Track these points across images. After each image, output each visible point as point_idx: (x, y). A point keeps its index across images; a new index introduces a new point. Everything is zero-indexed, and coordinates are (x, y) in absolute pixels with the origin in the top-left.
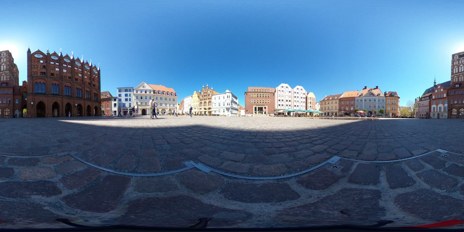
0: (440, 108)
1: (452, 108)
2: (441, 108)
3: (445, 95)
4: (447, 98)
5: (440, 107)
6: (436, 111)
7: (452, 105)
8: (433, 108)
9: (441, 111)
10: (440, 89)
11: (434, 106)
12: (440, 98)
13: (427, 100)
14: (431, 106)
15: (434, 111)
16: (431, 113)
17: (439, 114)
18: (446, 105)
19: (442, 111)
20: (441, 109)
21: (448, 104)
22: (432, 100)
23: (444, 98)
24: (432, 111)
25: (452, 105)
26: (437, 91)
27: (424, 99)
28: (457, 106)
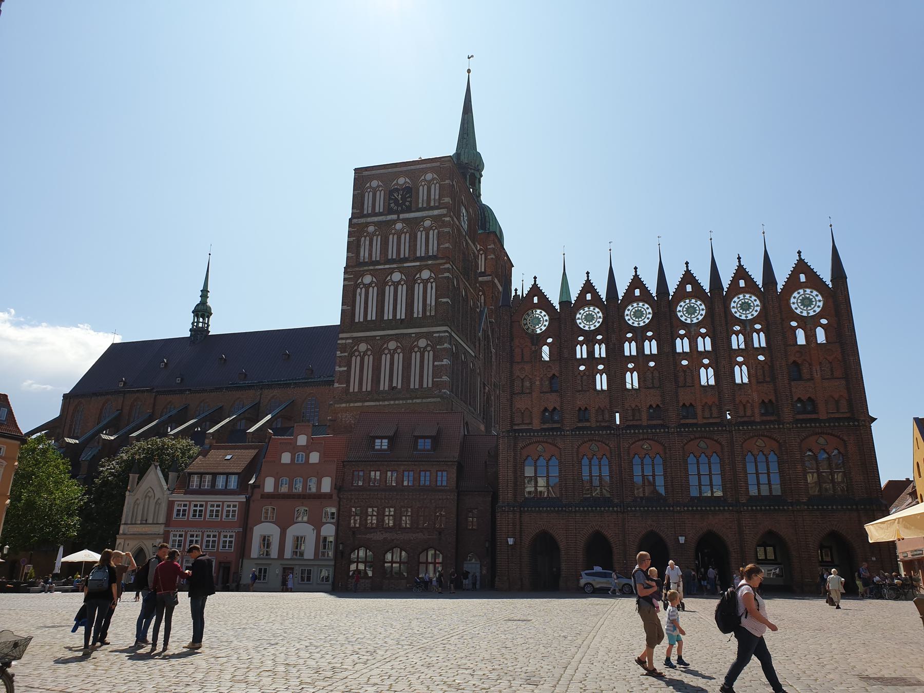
0: (299, 540)
3: (327, 485)
4: (335, 497)
6: (274, 553)
9: (302, 554)
10: (308, 449)
12: (304, 497)
13: (226, 492)
22: (257, 496)
24: (255, 551)
25: (354, 533)
26: (293, 459)
27: (207, 485)
28: (378, 536)
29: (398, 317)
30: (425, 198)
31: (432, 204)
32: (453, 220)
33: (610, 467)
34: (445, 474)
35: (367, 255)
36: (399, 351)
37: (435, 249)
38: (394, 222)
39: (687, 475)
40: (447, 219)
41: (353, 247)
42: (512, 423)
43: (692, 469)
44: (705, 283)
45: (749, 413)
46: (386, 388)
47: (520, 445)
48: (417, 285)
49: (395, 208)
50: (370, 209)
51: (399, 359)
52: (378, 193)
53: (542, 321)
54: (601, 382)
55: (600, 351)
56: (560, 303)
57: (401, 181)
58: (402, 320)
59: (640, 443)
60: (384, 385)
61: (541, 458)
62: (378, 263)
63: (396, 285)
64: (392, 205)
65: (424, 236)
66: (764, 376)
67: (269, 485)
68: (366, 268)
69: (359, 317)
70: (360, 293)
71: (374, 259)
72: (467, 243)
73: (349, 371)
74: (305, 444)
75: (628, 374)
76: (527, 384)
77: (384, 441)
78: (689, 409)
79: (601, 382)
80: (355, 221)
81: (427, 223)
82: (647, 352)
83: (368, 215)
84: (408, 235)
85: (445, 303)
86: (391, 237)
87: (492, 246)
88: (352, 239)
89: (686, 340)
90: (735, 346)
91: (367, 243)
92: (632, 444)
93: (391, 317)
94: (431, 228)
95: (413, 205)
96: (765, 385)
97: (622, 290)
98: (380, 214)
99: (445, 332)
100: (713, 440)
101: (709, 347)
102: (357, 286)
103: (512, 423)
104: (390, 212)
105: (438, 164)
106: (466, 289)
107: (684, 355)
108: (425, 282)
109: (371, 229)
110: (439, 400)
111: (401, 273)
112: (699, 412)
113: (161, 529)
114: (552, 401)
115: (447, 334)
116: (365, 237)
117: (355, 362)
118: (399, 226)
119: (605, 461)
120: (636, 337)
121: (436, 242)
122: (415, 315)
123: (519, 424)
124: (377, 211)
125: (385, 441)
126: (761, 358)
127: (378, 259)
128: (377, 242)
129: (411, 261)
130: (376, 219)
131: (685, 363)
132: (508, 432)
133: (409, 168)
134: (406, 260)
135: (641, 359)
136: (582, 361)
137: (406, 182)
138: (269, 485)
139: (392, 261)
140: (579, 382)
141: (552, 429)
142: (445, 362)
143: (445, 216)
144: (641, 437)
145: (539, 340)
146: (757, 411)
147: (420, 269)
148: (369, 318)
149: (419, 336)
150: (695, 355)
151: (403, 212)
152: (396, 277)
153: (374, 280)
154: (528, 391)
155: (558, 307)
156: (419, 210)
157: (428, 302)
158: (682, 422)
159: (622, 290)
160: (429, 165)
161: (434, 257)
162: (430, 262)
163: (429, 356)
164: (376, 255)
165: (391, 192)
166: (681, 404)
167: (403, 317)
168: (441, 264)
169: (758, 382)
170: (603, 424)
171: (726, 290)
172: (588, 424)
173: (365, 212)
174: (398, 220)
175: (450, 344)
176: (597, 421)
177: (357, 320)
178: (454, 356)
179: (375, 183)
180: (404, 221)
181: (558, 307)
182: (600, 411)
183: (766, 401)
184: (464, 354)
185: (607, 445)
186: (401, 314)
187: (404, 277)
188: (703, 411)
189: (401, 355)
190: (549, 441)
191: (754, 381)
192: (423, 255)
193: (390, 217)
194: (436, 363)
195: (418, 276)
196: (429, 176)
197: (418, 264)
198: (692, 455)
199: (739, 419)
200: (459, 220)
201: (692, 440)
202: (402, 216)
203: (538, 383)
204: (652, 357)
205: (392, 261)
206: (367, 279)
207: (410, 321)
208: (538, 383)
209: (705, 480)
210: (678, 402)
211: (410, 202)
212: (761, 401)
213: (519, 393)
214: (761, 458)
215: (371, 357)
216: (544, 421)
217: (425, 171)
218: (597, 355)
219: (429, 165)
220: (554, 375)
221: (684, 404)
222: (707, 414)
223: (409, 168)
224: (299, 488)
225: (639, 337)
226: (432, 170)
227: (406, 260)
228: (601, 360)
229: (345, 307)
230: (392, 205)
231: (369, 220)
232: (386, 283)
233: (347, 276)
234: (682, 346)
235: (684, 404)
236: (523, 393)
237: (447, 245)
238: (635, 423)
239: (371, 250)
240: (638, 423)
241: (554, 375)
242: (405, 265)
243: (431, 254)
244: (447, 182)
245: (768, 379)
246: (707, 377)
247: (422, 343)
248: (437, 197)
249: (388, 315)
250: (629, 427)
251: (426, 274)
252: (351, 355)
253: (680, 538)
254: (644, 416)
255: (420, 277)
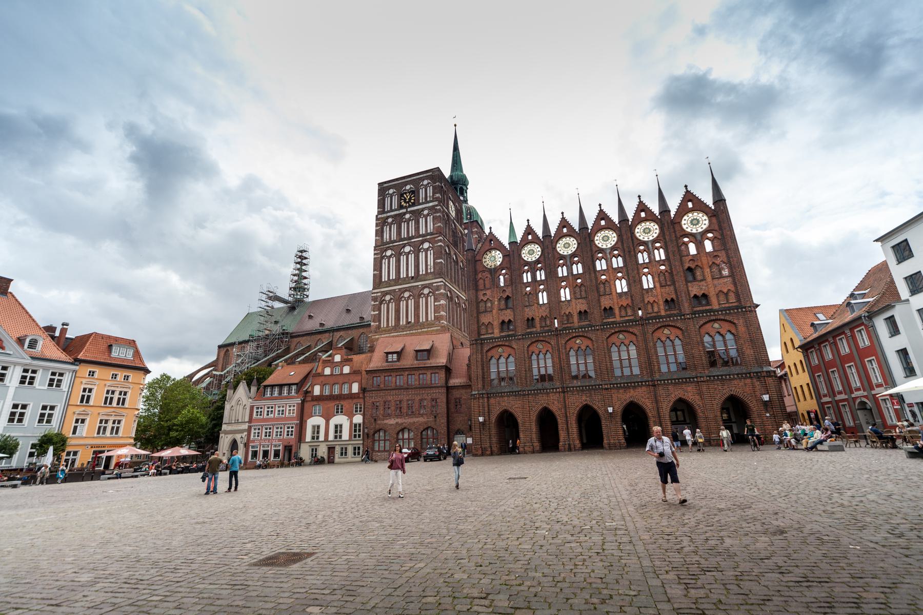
0: (339, 429)
1: (377, 427)
2: (341, 426)
3: (355, 388)
4: (361, 396)
5: (336, 426)
6: (322, 438)
7: (375, 420)
8: (314, 427)
9: (341, 437)
11: (315, 421)
14: (306, 421)
15: (315, 437)
16: (302, 444)
17: (334, 447)
18: (358, 419)
19: (343, 438)
20: (341, 432)
21: (364, 415)
22: (309, 399)
23: (351, 396)
24: (308, 438)
25: (375, 420)
26: (332, 371)
29: (410, 275)
30: (424, 196)
31: (428, 199)
32: (443, 208)
33: (553, 359)
34: (437, 375)
35: (388, 237)
36: (411, 298)
37: (432, 228)
38: (405, 214)
39: (611, 361)
40: (439, 207)
41: (379, 233)
42: (479, 334)
43: (615, 356)
44: (615, 218)
45: (656, 309)
46: (404, 323)
47: (486, 348)
48: (421, 253)
49: (405, 205)
50: (389, 207)
51: (411, 303)
52: (394, 197)
53: (495, 258)
54: (543, 298)
55: (541, 275)
56: (509, 244)
57: (408, 187)
58: (412, 278)
59: (573, 340)
60: (403, 322)
61: (502, 358)
62: (395, 241)
63: (408, 254)
64: (403, 203)
65: (424, 221)
66: (666, 281)
67: (317, 390)
68: (388, 246)
69: (385, 278)
70: (385, 262)
71: (392, 239)
72: (455, 225)
73: (380, 314)
74: (339, 360)
75: (562, 290)
76: (489, 305)
77: (394, 355)
78: (609, 311)
79: (543, 298)
80: (380, 216)
81: (426, 212)
82: (575, 272)
83: (388, 212)
84: (413, 222)
85: (439, 262)
86: (403, 224)
87: (476, 229)
88: (378, 228)
89: (603, 261)
90: (641, 261)
91: (388, 229)
92: (568, 340)
93: (405, 276)
94: (428, 215)
95: (416, 202)
96: (667, 287)
97: (553, 230)
98: (396, 210)
99: (441, 282)
100: (629, 332)
101: (621, 264)
102: (382, 258)
103: (479, 334)
104: (401, 207)
105: (431, 173)
106: (455, 254)
107: (603, 272)
108: (426, 250)
109: (390, 220)
110: (439, 328)
111: (410, 246)
112: (617, 311)
113: (245, 426)
114: (508, 315)
115: (442, 283)
116: (387, 226)
117: (384, 307)
118: (407, 216)
119: (549, 355)
120: (566, 262)
121: (432, 224)
122: (421, 273)
123: (484, 335)
124: (393, 208)
125: (396, 355)
126: (663, 268)
127: (395, 239)
128: (394, 228)
129: (416, 238)
130: (392, 213)
131: (604, 277)
132: (476, 340)
133: (412, 178)
134: (413, 237)
135: (572, 277)
136: (528, 284)
137: (411, 188)
138: (317, 390)
139: (405, 239)
140: (527, 299)
141: (509, 336)
142: (442, 302)
143: (437, 205)
144: (574, 335)
145: (495, 272)
146: (662, 307)
147: (422, 242)
148: (391, 278)
149: (424, 287)
150: (611, 270)
151: (410, 206)
152: (407, 249)
153: (393, 253)
154: (489, 310)
155: (508, 247)
156: (420, 204)
157: (429, 263)
158: (605, 321)
159: (553, 230)
160: (425, 175)
161: (431, 234)
162: (428, 237)
163: (431, 299)
164: (394, 236)
165: (402, 195)
166: (603, 308)
167: (413, 275)
168: (436, 237)
169: (661, 286)
170: (546, 329)
171: (631, 220)
172: (534, 330)
173: (386, 210)
174: (407, 212)
175: (445, 290)
176: (541, 327)
177: (383, 280)
178: (450, 299)
179: (391, 191)
180: (411, 212)
181: (508, 247)
182: (543, 319)
183: (669, 299)
184: (457, 297)
185: (549, 343)
186: (412, 273)
187: (412, 249)
188: (620, 311)
189: (413, 300)
190: (507, 344)
191: (658, 285)
192: (424, 233)
193: (401, 211)
194: (436, 304)
195: (421, 247)
196: (425, 182)
197: (421, 239)
198: (614, 345)
199: (649, 316)
200: (448, 209)
201: (613, 334)
202: (409, 210)
203: (496, 303)
204: (578, 276)
205: (405, 239)
206: (389, 253)
207: (417, 277)
208: (496, 303)
209: (626, 363)
210: (600, 306)
211: (414, 200)
212: (664, 300)
213: (483, 312)
214: (668, 343)
215: (394, 303)
216: (502, 330)
217: (423, 179)
218: (539, 279)
219: (425, 175)
220: (508, 296)
221: (605, 308)
222: (623, 313)
223: (412, 178)
224: (336, 391)
225: (568, 263)
226: (426, 178)
227: (413, 237)
228: (542, 282)
229: (376, 272)
230: (403, 203)
231: (389, 214)
232: (400, 254)
233: (376, 252)
234: (601, 265)
235: (605, 308)
236: (486, 311)
237: (439, 224)
238: (569, 325)
239: (390, 233)
240: (572, 325)
241: (508, 296)
242: (413, 240)
243: (429, 232)
244: (437, 184)
245: (668, 283)
246: (621, 286)
247: (426, 291)
248: (431, 195)
249: (403, 275)
250: (565, 329)
251: (426, 245)
252: (381, 303)
253: (609, 408)
254: (576, 318)
255: (423, 247)
